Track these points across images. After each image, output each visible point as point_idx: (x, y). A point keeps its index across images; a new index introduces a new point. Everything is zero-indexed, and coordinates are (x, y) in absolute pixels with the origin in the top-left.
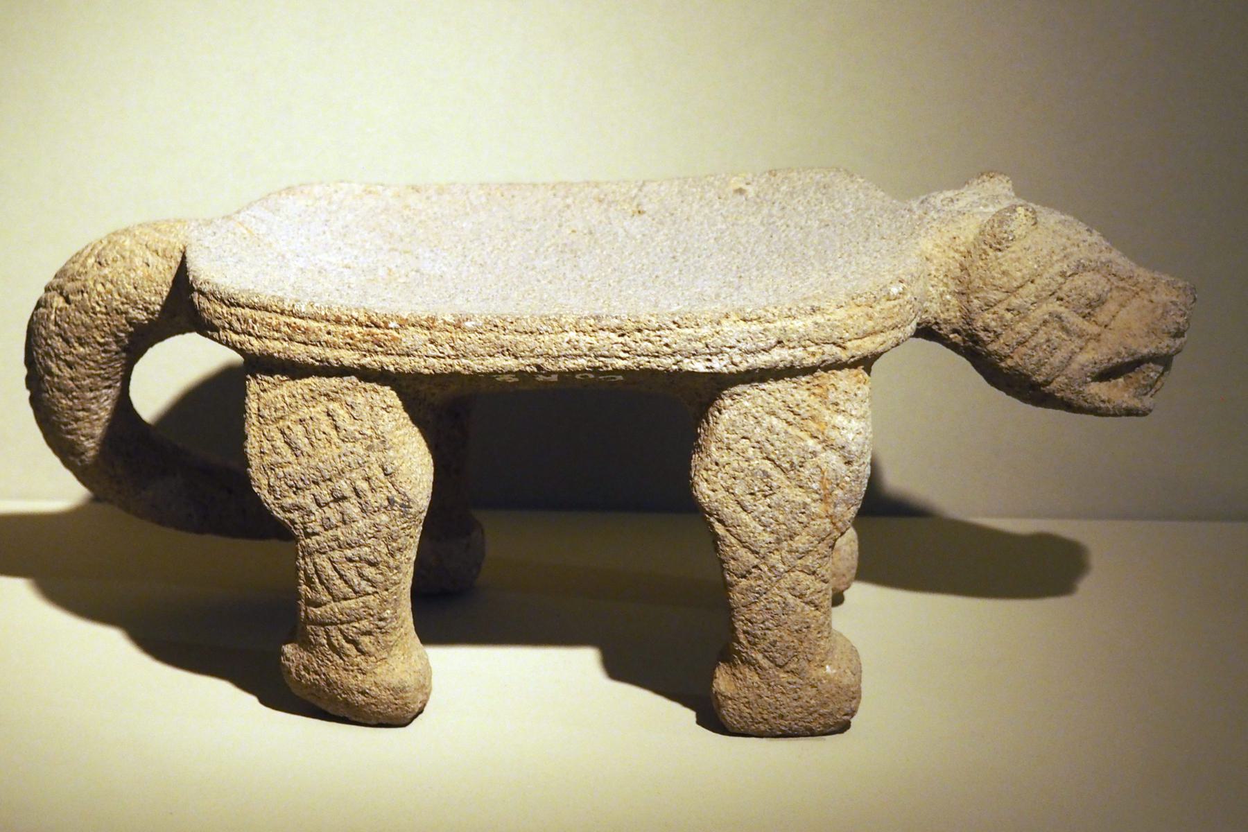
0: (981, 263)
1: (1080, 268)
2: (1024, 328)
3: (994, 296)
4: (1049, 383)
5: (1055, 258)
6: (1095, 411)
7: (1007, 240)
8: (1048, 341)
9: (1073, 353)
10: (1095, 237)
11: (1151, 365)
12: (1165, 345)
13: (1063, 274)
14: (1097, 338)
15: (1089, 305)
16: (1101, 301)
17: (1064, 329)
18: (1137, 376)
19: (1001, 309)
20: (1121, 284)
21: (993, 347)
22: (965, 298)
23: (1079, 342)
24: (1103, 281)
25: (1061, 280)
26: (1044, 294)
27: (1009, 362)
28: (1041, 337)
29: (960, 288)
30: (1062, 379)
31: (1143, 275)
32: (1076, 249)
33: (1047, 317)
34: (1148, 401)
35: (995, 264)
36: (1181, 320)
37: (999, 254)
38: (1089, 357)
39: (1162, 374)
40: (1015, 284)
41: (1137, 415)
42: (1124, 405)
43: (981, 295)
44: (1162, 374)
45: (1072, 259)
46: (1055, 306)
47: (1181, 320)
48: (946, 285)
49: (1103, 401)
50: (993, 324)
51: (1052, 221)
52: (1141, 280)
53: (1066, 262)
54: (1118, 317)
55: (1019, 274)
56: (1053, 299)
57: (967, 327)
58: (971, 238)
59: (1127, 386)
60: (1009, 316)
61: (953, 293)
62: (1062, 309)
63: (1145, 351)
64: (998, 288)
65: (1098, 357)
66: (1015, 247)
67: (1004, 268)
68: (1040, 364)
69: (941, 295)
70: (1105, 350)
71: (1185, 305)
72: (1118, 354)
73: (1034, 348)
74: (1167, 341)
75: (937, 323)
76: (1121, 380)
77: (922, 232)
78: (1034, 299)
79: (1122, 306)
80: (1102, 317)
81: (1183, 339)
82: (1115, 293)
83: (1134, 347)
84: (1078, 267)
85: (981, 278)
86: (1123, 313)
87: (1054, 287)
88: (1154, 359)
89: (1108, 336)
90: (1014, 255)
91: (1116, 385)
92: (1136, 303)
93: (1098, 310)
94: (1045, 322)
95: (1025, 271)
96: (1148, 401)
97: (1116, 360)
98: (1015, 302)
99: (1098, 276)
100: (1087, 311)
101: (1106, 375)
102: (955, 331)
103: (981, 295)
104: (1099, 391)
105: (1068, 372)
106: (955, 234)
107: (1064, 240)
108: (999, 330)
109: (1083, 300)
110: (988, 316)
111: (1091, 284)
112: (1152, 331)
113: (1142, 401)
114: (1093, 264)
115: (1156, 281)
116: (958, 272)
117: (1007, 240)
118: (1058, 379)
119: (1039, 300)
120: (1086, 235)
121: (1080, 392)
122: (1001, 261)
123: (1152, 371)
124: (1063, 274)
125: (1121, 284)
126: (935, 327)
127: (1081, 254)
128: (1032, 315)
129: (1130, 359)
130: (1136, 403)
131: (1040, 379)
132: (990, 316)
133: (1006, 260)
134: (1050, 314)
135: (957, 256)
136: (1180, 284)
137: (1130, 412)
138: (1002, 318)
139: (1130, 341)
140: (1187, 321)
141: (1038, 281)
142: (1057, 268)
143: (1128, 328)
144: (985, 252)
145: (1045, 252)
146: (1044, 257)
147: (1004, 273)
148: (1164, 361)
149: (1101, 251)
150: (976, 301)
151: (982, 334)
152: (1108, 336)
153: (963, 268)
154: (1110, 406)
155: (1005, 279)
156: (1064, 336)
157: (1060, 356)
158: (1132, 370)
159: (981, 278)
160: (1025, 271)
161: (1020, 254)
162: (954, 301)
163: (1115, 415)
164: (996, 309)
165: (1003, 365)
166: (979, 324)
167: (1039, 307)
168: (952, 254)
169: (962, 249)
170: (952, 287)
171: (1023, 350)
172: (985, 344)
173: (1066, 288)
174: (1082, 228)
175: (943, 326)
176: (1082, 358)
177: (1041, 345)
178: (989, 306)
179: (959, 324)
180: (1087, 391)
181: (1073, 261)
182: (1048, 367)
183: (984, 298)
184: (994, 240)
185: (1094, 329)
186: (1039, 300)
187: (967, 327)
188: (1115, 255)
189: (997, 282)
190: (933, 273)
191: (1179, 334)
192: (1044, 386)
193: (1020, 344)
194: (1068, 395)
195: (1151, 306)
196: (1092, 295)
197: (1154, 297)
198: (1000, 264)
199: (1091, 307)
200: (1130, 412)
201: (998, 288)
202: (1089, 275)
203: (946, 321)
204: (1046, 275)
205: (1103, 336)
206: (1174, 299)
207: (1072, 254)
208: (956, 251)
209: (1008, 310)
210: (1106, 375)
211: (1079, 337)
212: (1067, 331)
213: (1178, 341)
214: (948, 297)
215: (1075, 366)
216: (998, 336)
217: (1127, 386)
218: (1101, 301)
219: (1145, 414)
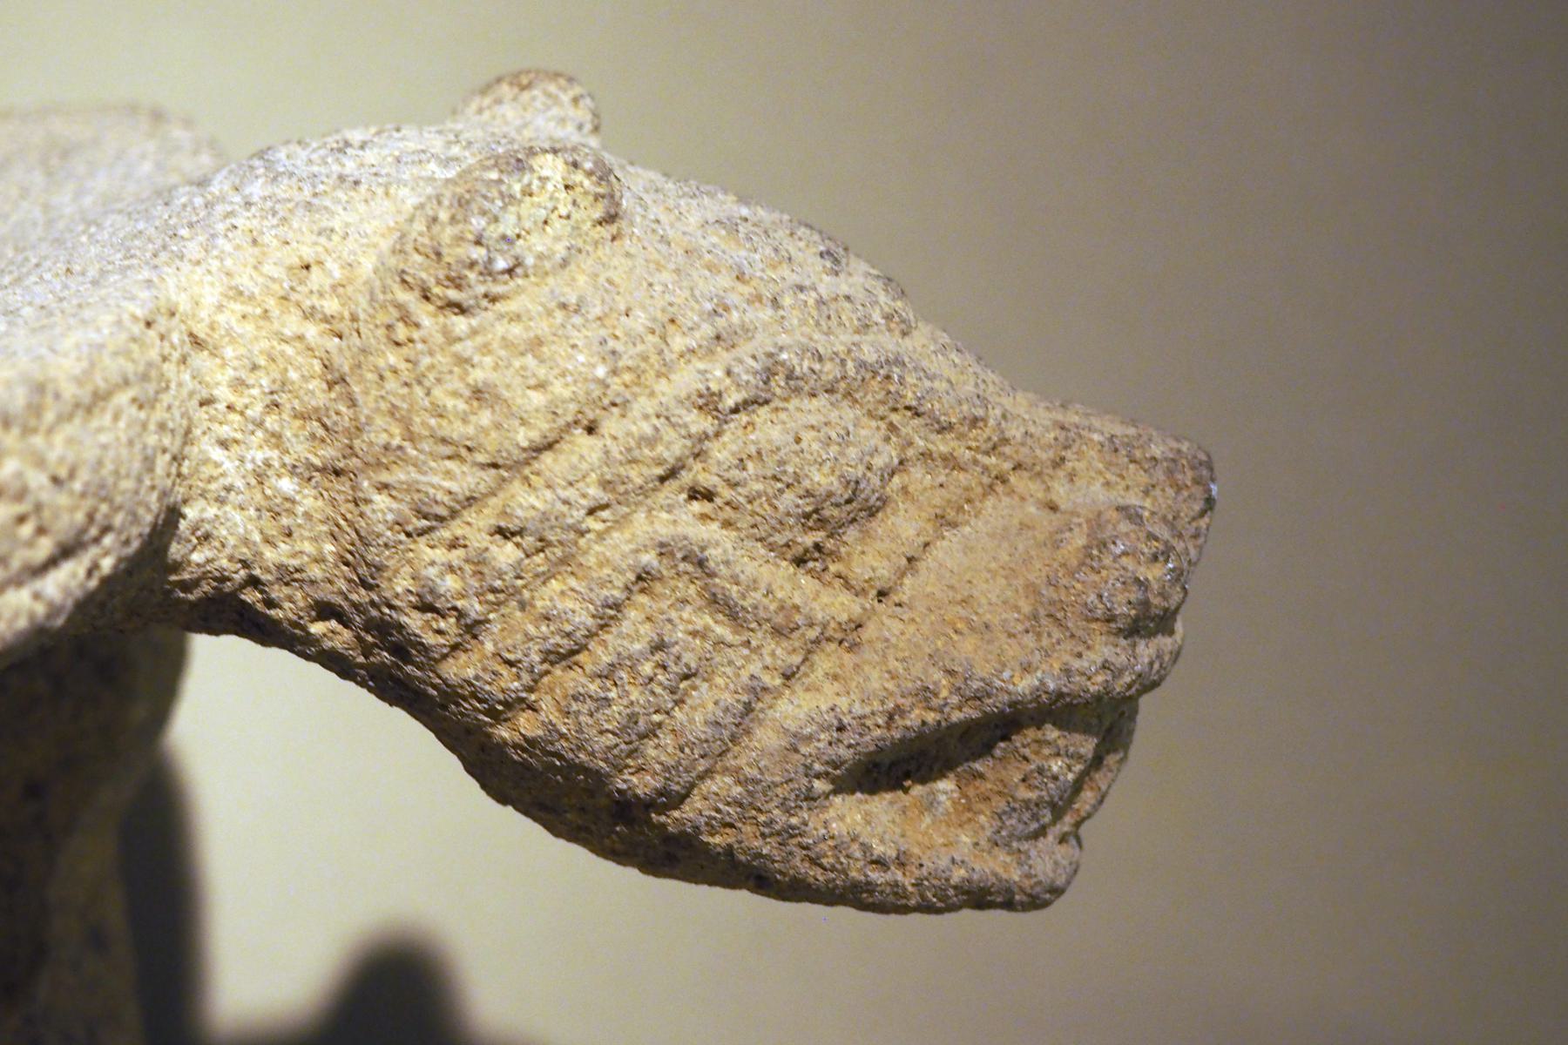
0: (393, 358)
1: (775, 383)
2: (566, 600)
3: (447, 480)
4: (680, 799)
5: (678, 342)
6: (857, 896)
7: (488, 272)
8: (659, 646)
9: (758, 691)
10: (857, 278)
11: (1052, 733)
12: (1095, 662)
13: (708, 402)
14: (849, 635)
15: (814, 518)
16: (861, 506)
17: (717, 602)
18: (1001, 771)
19: (475, 527)
20: (942, 445)
21: (459, 669)
22: (342, 486)
23: (782, 653)
24: (869, 434)
25: (700, 423)
26: (636, 475)
27: (526, 725)
28: (633, 634)
29: (328, 453)
30: (720, 784)
31: (1027, 416)
32: (766, 314)
33: (649, 558)
34: (1047, 859)
35: (442, 359)
36: (1154, 574)
37: (460, 324)
38: (818, 705)
39: (1097, 762)
40: (523, 437)
41: (1009, 905)
42: (958, 875)
43: (398, 476)
44: (1097, 762)
45: (745, 350)
46: (684, 522)
47: (1154, 574)
48: (276, 439)
49: (880, 863)
50: (450, 583)
51: (693, 220)
52: (1014, 432)
53: (724, 357)
54: (927, 563)
55: (537, 398)
56: (671, 493)
57: (361, 596)
58: (367, 265)
59: (966, 810)
60: (506, 554)
61: (305, 473)
62: (713, 530)
63: (1024, 685)
64: (459, 451)
65: (849, 705)
66: (526, 298)
67: (477, 376)
68: (638, 732)
69: (260, 477)
70: (876, 680)
71: (1171, 523)
72: (925, 694)
73: (607, 675)
74: (1104, 649)
75: (254, 582)
76: (946, 786)
77: (193, 249)
78: (595, 492)
79: (943, 521)
80: (869, 556)
81: (1165, 642)
82: (917, 475)
83: (983, 670)
84: (769, 374)
85: (393, 411)
86: (947, 551)
87: (673, 447)
88: (1058, 710)
89: (886, 625)
90: (516, 330)
91: (930, 805)
92: (996, 511)
93: (851, 534)
94: (644, 579)
95: (558, 388)
96: (1047, 859)
97: (914, 718)
98: (526, 502)
99: (849, 414)
100: (809, 540)
101: (889, 767)
102: (325, 611)
103: (398, 476)
104: (864, 823)
105: (742, 759)
106: (308, 253)
107: (725, 280)
108: (474, 608)
109: (788, 500)
110: (431, 555)
111: (816, 441)
112: (1048, 614)
113: (1021, 857)
114: (830, 370)
115: (1068, 437)
116: (317, 394)
117: (488, 272)
118: (710, 786)
119: (615, 499)
120: (812, 268)
121: (790, 832)
122: (466, 348)
123: (1057, 755)
124: (708, 402)
125: (942, 445)
126: (251, 596)
127: (786, 334)
128: (593, 553)
129: (970, 713)
130: (999, 867)
131: (643, 784)
132: (440, 554)
133: (489, 343)
134: (664, 550)
135: (312, 331)
136: (1156, 450)
137: (979, 897)
138: (479, 562)
139: (968, 646)
140: (1178, 575)
141: (611, 425)
142: (686, 379)
143: (968, 600)
144: (406, 318)
145: (640, 321)
146: (636, 338)
147: (478, 394)
148: (1106, 720)
149: (865, 327)
150: (381, 500)
151: (414, 622)
152: (886, 625)
153: (336, 381)
154: (908, 882)
155: (485, 418)
156: (723, 631)
157: (706, 705)
158: (986, 750)
159: (393, 411)
160: (558, 388)
161: (542, 327)
162: (309, 501)
163: (926, 908)
164: (456, 529)
165: (503, 732)
166: (402, 584)
167: (621, 523)
168: (292, 324)
169: (331, 306)
170: (300, 449)
171: (569, 680)
172: (431, 659)
173: (722, 452)
174: (806, 252)
175: (277, 593)
176: (794, 710)
177: (633, 663)
178: (430, 519)
179: (337, 589)
180: (815, 827)
181: (747, 359)
182: (667, 740)
183: (411, 487)
184: (452, 279)
185: (837, 605)
186: (615, 499)
187: (361, 596)
188: (921, 343)
189: (456, 430)
190: (224, 394)
191: (1149, 621)
192: (663, 809)
193: (555, 657)
194: (749, 840)
195: (1047, 521)
196: (821, 479)
197: (1060, 491)
198: (463, 361)
199: (823, 527)
200: (979, 897)
201: (459, 451)
202: (815, 409)
203: (287, 576)
204: (643, 404)
205: (870, 632)
206: (1133, 499)
207: (747, 331)
208: (309, 314)
209: (503, 533)
210: (889, 767)
211: (778, 632)
212: (733, 614)
213: (1146, 650)
214: (287, 485)
215: (765, 738)
216: (472, 629)
217: (966, 810)
218: (861, 506)
219: (1035, 903)
